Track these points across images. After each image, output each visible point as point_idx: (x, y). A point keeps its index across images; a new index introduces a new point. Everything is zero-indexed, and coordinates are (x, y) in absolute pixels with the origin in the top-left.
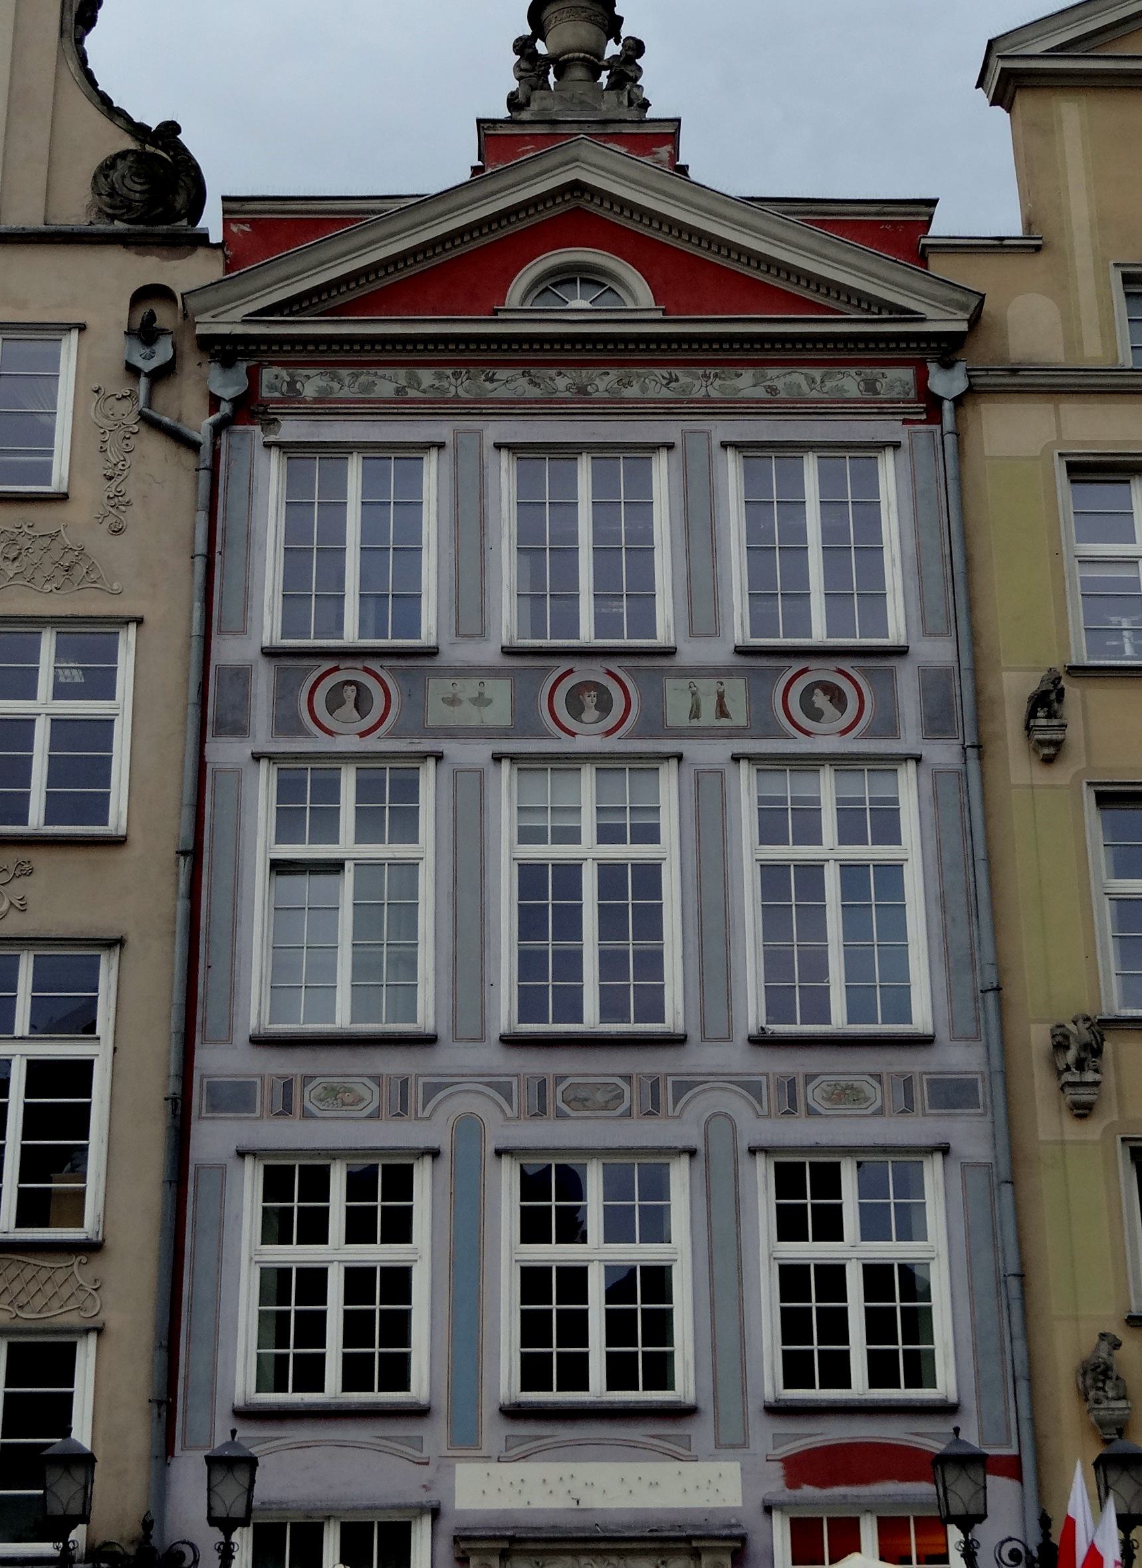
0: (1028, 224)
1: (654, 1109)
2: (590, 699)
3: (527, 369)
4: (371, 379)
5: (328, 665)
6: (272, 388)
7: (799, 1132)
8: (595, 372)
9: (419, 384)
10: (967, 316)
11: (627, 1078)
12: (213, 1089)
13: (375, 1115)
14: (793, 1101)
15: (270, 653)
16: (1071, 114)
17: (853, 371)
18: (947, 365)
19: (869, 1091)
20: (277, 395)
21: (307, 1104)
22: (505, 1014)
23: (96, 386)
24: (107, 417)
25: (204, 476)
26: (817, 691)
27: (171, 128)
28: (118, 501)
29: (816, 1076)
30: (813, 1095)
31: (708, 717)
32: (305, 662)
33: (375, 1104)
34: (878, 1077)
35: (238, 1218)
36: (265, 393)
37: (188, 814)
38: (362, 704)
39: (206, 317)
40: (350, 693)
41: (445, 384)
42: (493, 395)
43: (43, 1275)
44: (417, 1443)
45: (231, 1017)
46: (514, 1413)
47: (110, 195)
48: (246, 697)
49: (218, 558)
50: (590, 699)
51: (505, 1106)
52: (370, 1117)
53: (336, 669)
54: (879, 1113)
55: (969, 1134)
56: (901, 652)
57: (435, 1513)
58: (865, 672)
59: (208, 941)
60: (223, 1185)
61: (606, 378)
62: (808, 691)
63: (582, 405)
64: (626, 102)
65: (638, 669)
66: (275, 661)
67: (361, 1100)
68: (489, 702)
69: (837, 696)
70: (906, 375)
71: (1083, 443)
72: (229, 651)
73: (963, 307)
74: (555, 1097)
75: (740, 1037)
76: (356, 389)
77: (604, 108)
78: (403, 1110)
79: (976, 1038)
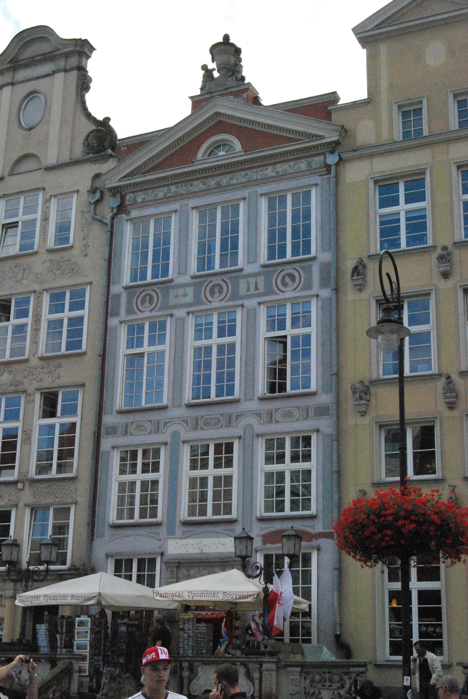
0: (369, 92)
1: (229, 424)
2: (216, 290)
6: (129, 201)
7: (273, 428)
9: (171, 191)
10: (338, 134)
11: (222, 415)
12: (107, 428)
13: (150, 433)
14: (271, 417)
15: (126, 288)
16: (383, 49)
17: (304, 161)
18: (332, 152)
19: (295, 413)
22: (188, 397)
25: (109, 233)
26: (287, 277)
27: (107, 120)
28: (86, 246)
29: (279, 409)
30: (277, 416)
31: (252, 291)
34: (298, 408)
36: (127, 203)
39: (108, 182)
40: (148, 298)
42: (193, 191)
43: (62, 487)
44: (158, 534)
46: (185, 524)
47: (88, 146)
48: (119, 304)
50: (216, 290)
51: (186, 427)
54: (298, 420)
55: (326, 425)
56: (314, 259)
58: (303, 268)
61: (226, 178)
62: (284, 278)
63: (219, 188)
64: (234, 79)
65: (232, 278)
68: (187, 295)
69: (292, 277)
70: (321, 158)
71: (379, 172)
72: (115, 289)
73: (336, 131)
74: (201, 422)
75: (256, 398)
76: (153, 196)
79: (331, 391)
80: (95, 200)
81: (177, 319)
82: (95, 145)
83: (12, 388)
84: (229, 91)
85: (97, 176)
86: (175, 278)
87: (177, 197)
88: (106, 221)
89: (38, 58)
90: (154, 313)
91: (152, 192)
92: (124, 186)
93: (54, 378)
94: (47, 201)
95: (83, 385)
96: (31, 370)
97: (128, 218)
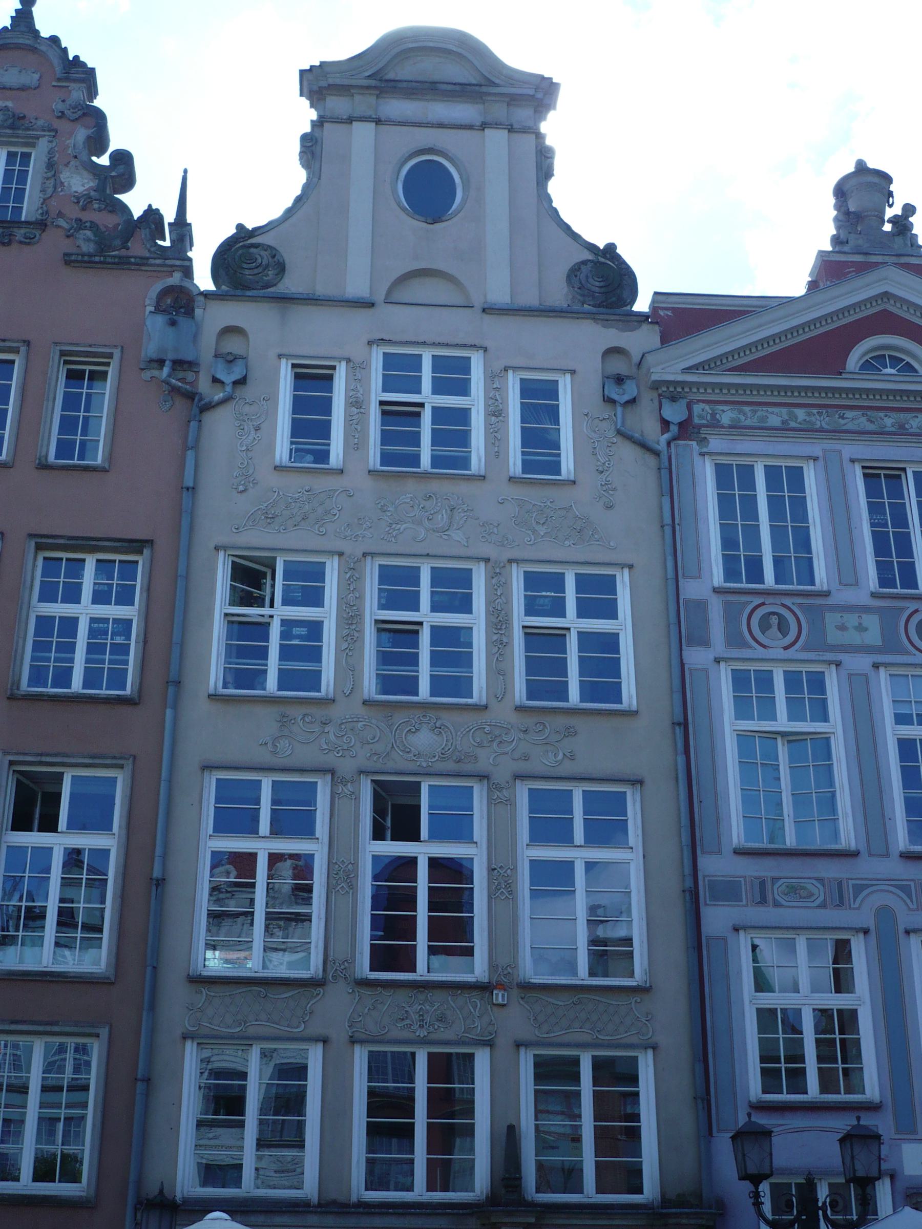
3: (865, 412)
4: (765, 414)
5: (757, 601)
8: (909, 415)
9: (796, 418)
13: (823, 906)
15: (717, 591)
20: (704, 422)
21: (777, 897)
23: (586, 411)
24: (595, 432)
25: (665, 473)
32: (743, 598)
33: (822, 898)
35: (740, 973)
36: (696, 421)
37: (677, 697)
38: (783, 628)
40: (774, 620)
41: (813, 419)
42: (844, 428)
45: (719, 837)
48: (706, 620)
49: (677, 527)
52: (819, 907)
53: (763, 604)
57: (892, 1177)
59: (698, 784)
60: (726, 953)
61: (917, 420)
66: (722, 597)
67: (812, 895)
68: (866, 629)
72: (692, 590)
76: (755, 420)
77: (896, 247)
78: (841, 903)
80: (626, 398)
81: (850, 675)
82: (597, 290)
83: (450, 766)
84: (903, 260)
85: (612, 352)
86: (833, 592)
87: (809, 431)
88: (659, 448)
89: (449, 87)
90: (791, 653)
91: (756, 412)
92: (691, 384)
93: (560, 757)
94: (494, 377)
95: (641, 782)
96: (497, 733)
97: (704, 450)
